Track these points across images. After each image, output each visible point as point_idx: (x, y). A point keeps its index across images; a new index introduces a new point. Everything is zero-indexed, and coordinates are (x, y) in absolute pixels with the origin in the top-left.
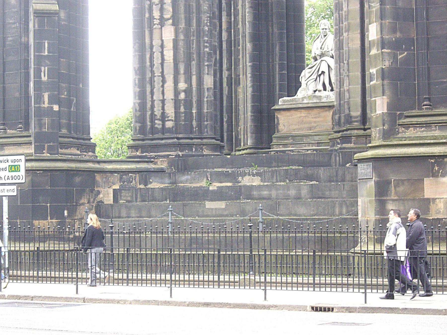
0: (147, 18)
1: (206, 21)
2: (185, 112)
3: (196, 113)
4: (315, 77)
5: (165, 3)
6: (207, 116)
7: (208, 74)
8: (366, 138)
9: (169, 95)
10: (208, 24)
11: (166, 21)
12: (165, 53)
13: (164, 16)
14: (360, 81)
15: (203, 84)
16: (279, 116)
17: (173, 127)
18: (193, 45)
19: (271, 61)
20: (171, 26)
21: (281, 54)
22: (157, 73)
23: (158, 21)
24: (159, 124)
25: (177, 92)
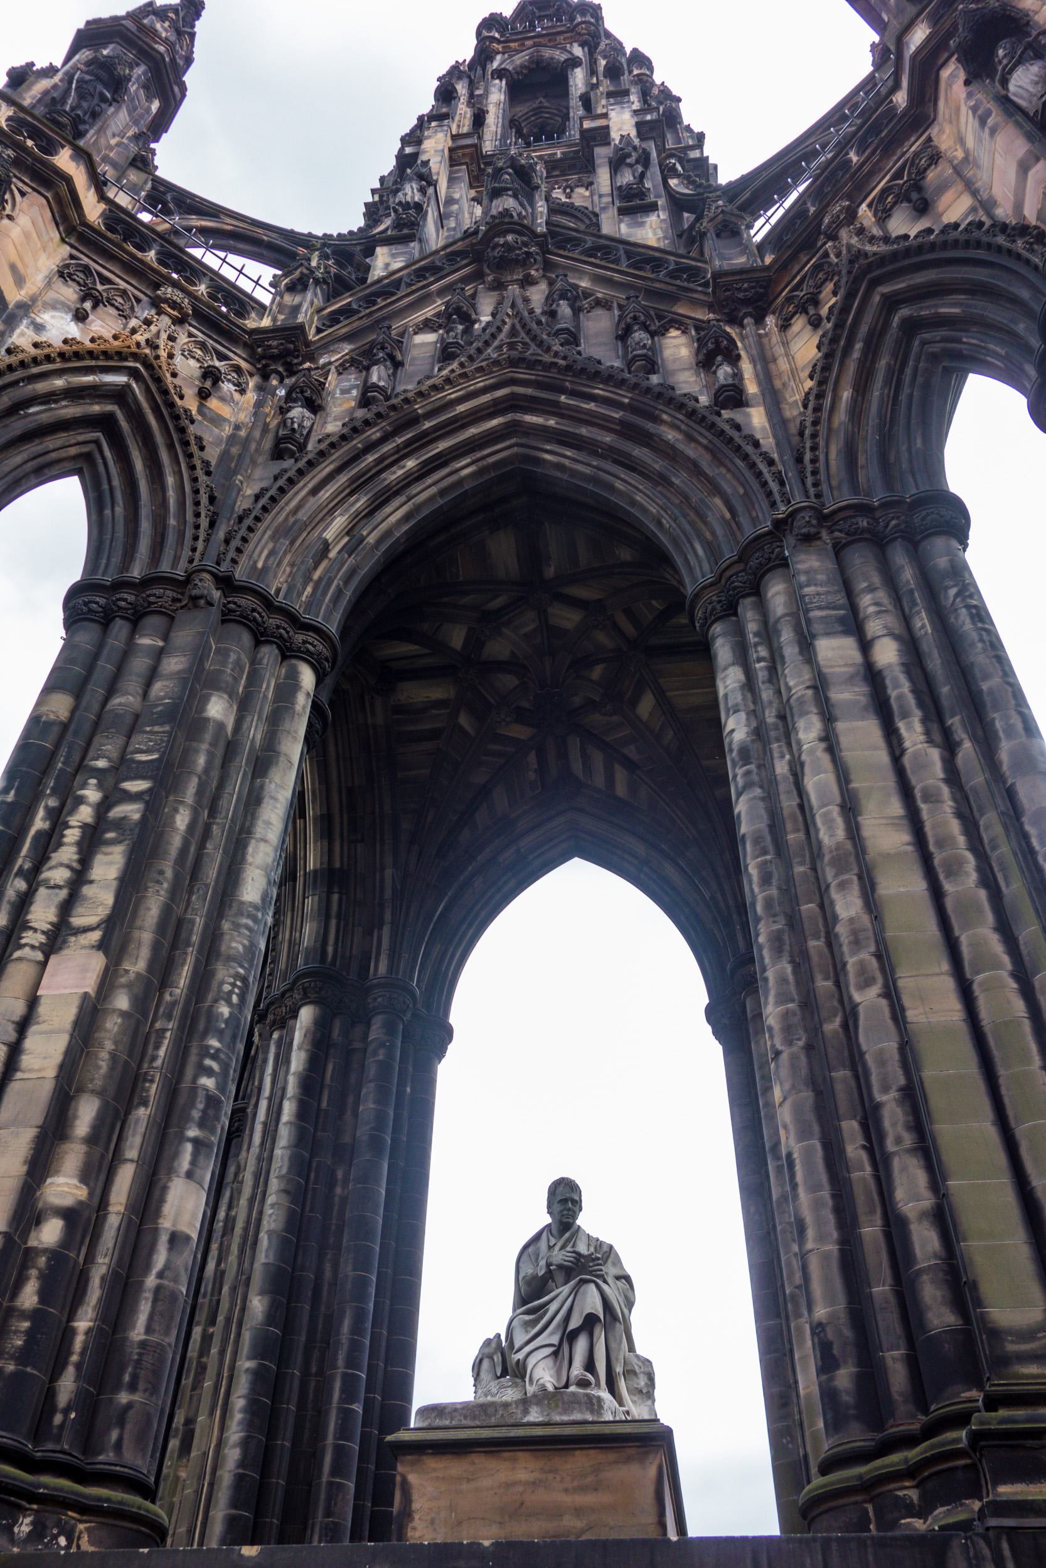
1: (227, 988)
2: (36, 1316)
3: (88, 1332)
4: (555, 1340)
5: (91, 882)
6: (138, 1362)
7: (189, 1175)
10: (235, 999)
11: (75, 934)
12: (29, 1043)
13: (72, 920)
14: (1001, 1159)
15: (158, 1213)
16: (412, 1478)
19: (314, 1370)
20: (94, 951)
21: (355, 1346)
23: (42, 938)
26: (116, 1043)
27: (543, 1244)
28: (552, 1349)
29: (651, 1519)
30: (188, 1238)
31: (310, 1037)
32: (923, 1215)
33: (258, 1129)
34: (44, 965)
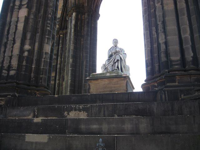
0: (11, 6)
1: (50, 12)
2: (26, 66)
3: (34, 67)
4: (112, 64)
6: (43, 71)
7: (47, 43)
8: (190, 77)
9: (16, 51)
11: (23, 6)
12: (18, 25)
14: (177, 33)
15: (43, 49)
17: (15, 75)
18: (39, 23)
21: (86, 65)
22: (11, 38)
23: (18, 7)
24: (5, 73)
25: (22, 50)
26: (32, 23)
27: (112, 49)
28: (111, 65)
29: (125, 88)
30: (48, 53)
31: (75, 18)
32: (163, 43)
33: (69, 33)
34: (19, 12)
